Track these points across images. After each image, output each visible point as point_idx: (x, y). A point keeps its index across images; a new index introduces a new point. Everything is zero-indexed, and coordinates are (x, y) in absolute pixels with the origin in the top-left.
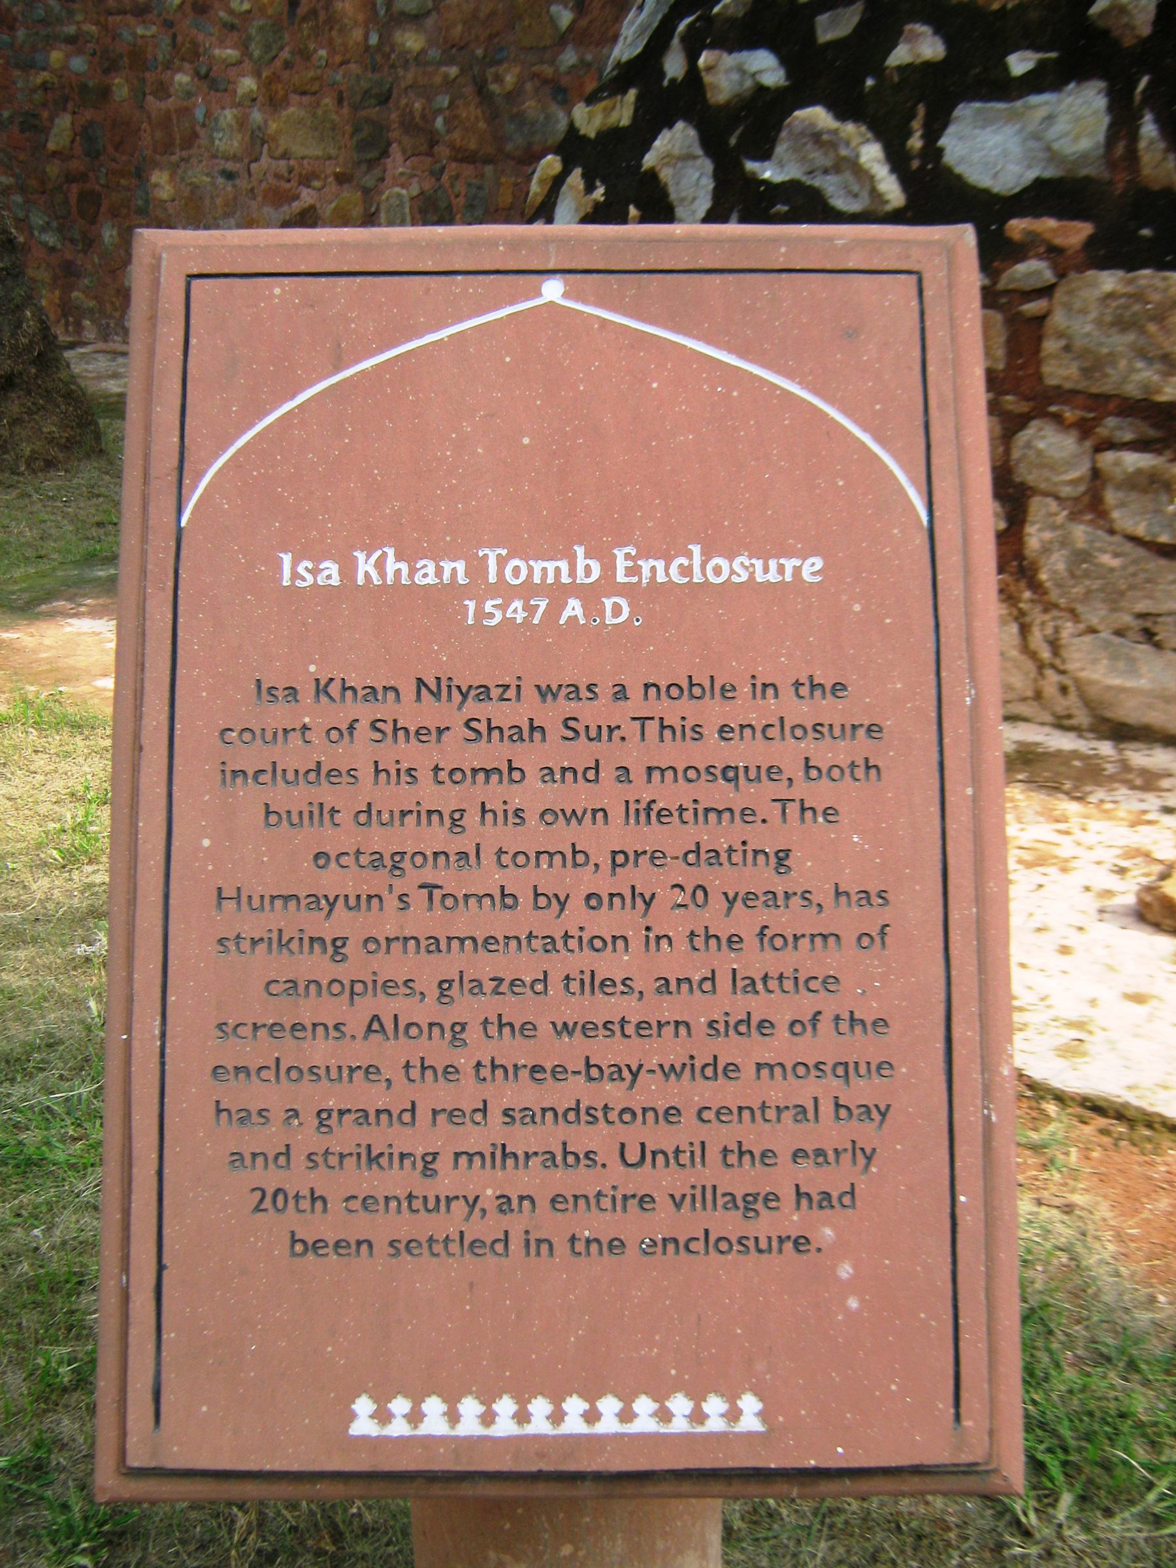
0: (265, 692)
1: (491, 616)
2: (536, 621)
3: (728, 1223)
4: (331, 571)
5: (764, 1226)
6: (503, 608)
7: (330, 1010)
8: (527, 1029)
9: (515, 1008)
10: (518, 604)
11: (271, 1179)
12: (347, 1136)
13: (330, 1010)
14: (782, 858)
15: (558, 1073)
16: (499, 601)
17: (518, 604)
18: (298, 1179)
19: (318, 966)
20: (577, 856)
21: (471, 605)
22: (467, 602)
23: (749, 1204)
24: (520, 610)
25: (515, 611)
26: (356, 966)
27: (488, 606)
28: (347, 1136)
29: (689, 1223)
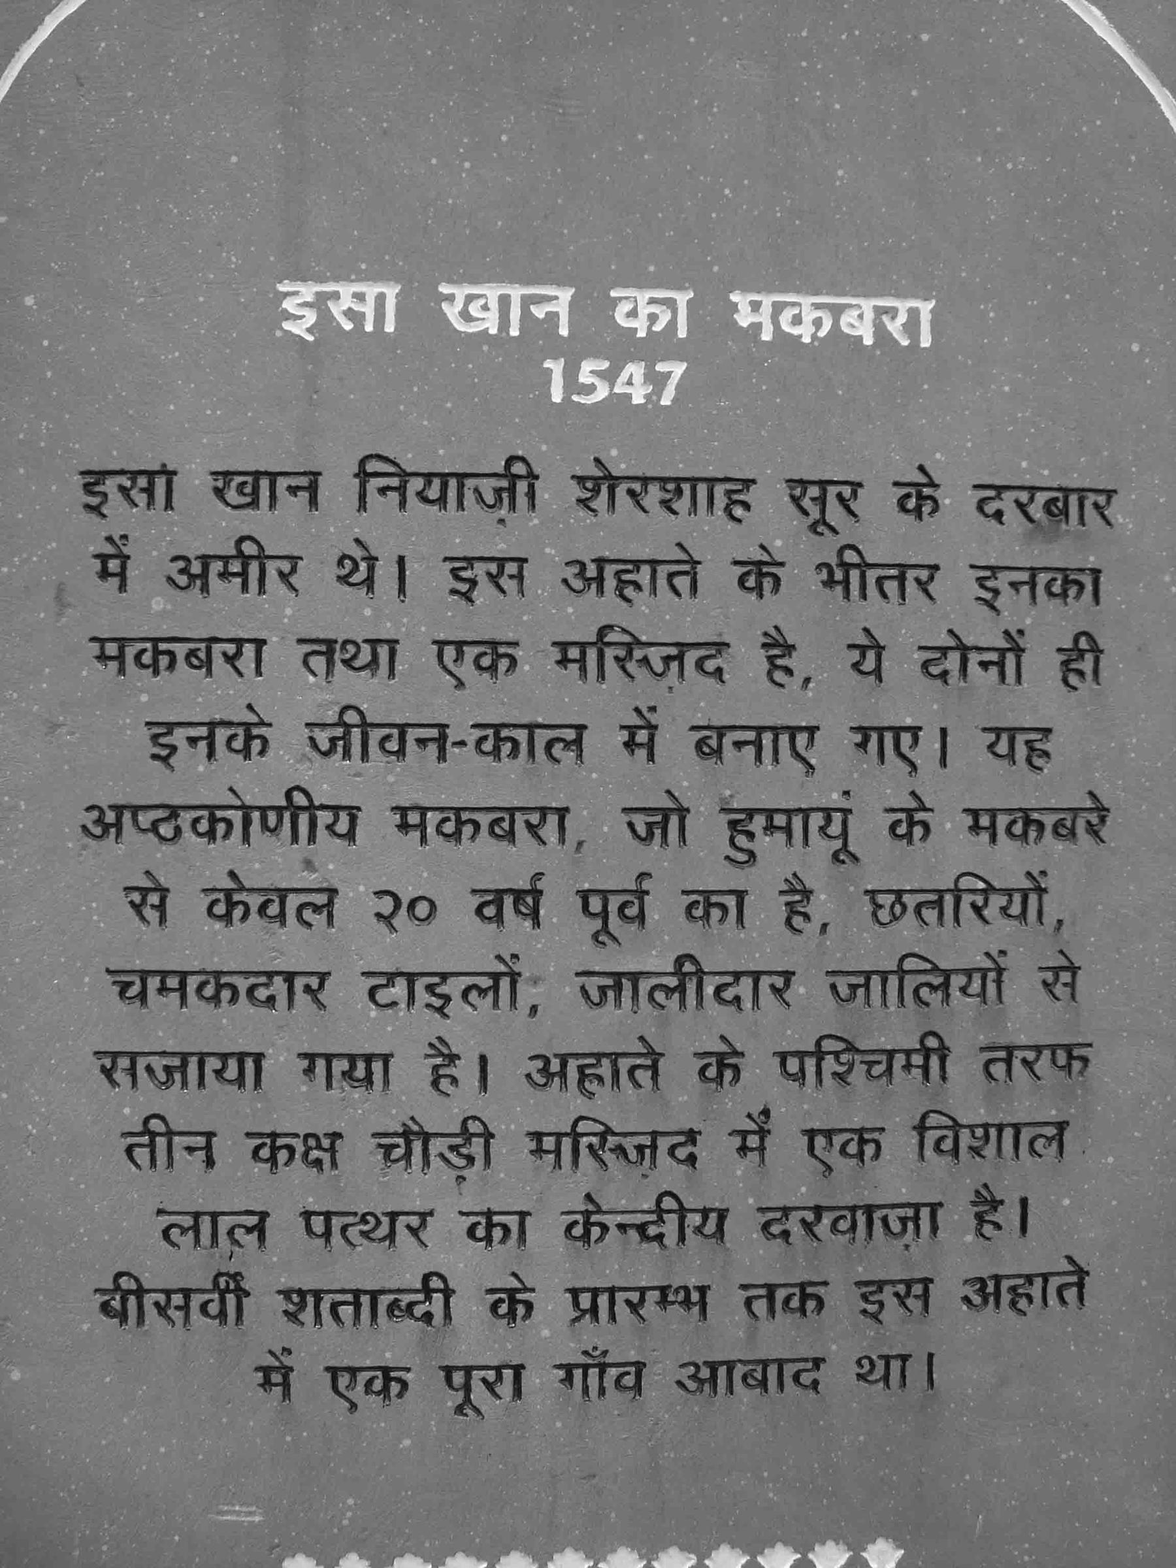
1: (591, 389)
2: (666, 401)
6: (610, 376)
10: (635, 370)
16: (605, 365)
17: (635, 370)
21: (556, 367)
22: (548, 364)
24: (638, 379)
25: (630, 383)
27: (587, 372)
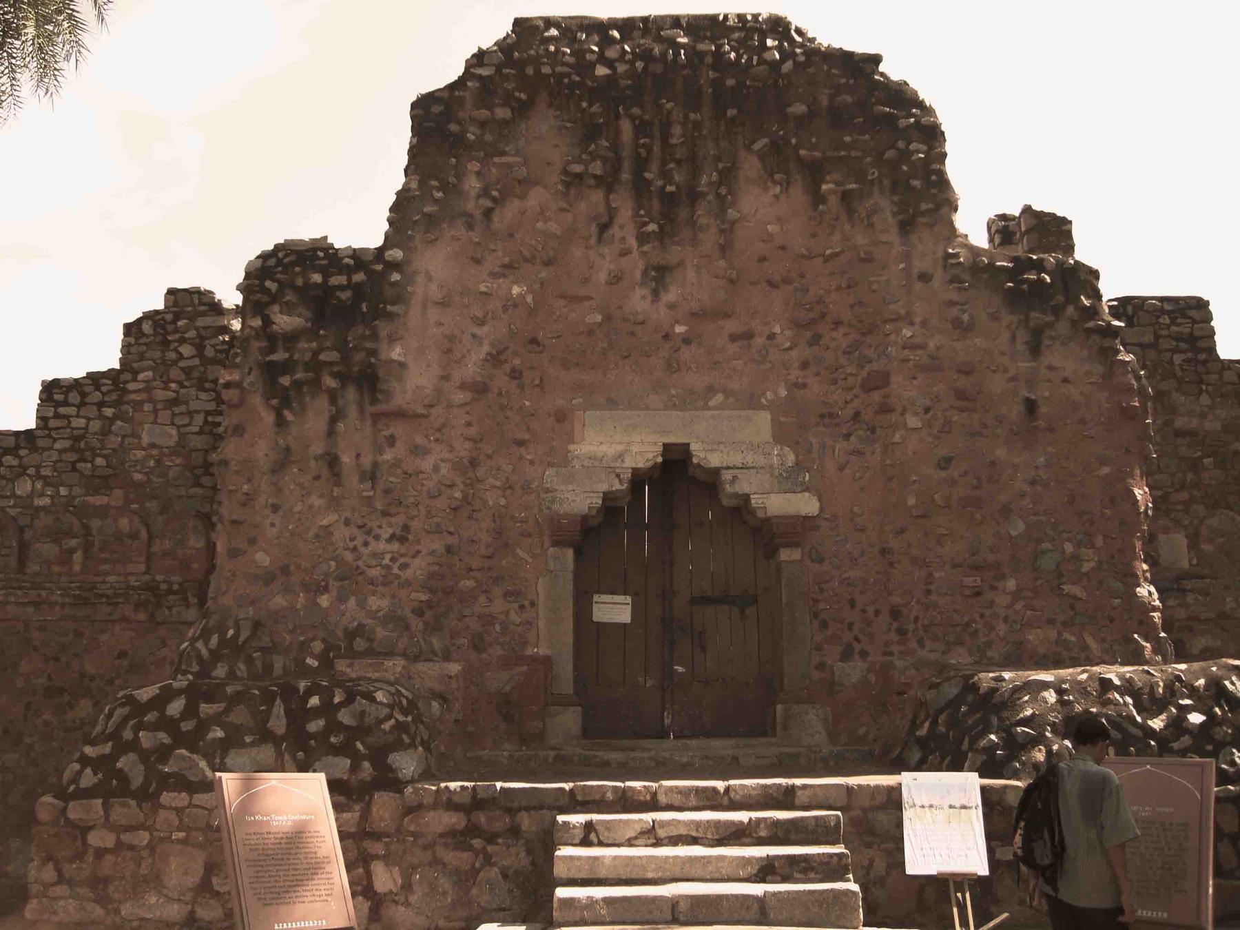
0: (247, 834)
3: (318, 899)
4: (252, 818)
5: (322, 898)
7: (263, 874)
8: (288, 875)
9: (287, 873)
11: (259, 896)
12: (267, 890)
13: (263, 874)
14: (316, 853)
15: (293, 881)
18: (262, 896)
19: (260, 869)
20: (290, 854)
23: (320, 896)
26: (265, 869)
28: (267, 890)
29: (313, 899)
